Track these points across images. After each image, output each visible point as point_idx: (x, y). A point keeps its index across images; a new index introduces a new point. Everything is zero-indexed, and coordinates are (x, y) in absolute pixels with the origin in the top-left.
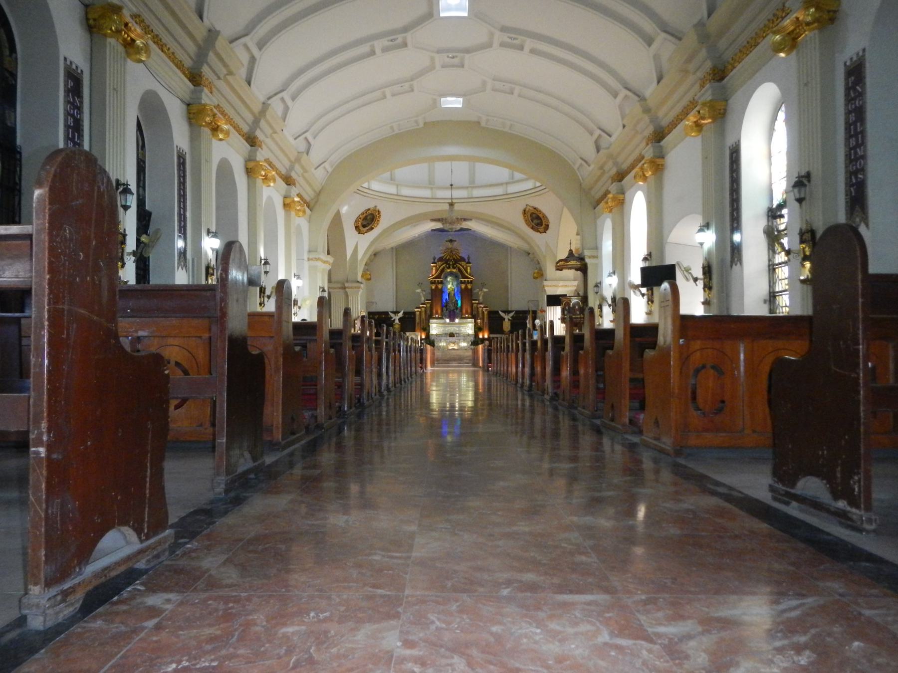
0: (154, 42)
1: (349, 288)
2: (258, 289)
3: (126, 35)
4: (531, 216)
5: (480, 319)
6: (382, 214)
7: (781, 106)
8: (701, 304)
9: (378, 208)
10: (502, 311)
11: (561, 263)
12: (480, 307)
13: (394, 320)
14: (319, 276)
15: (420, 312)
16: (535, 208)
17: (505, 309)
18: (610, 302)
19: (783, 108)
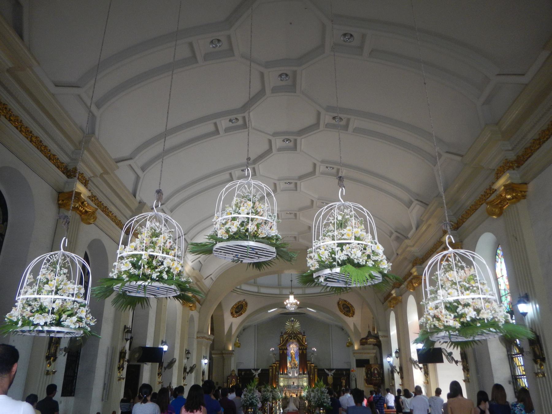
0: (103, 211)
1: (226, 354)
2: (158, 364)
3: (82, 209)
4: (342, 306)
5: (312, 375)
6: (249, 305)
7: (499, 246)
8: (463, 381)
9: (246, 300)
10: (326, 369)
11: (363, 340)
12: (312, 366)
13: (255, 375)
14: (204, 348)
15: (272, 369)
16: (345, 301)
17: (328, 368)
18: (398, 370)
19: (500, 248)
